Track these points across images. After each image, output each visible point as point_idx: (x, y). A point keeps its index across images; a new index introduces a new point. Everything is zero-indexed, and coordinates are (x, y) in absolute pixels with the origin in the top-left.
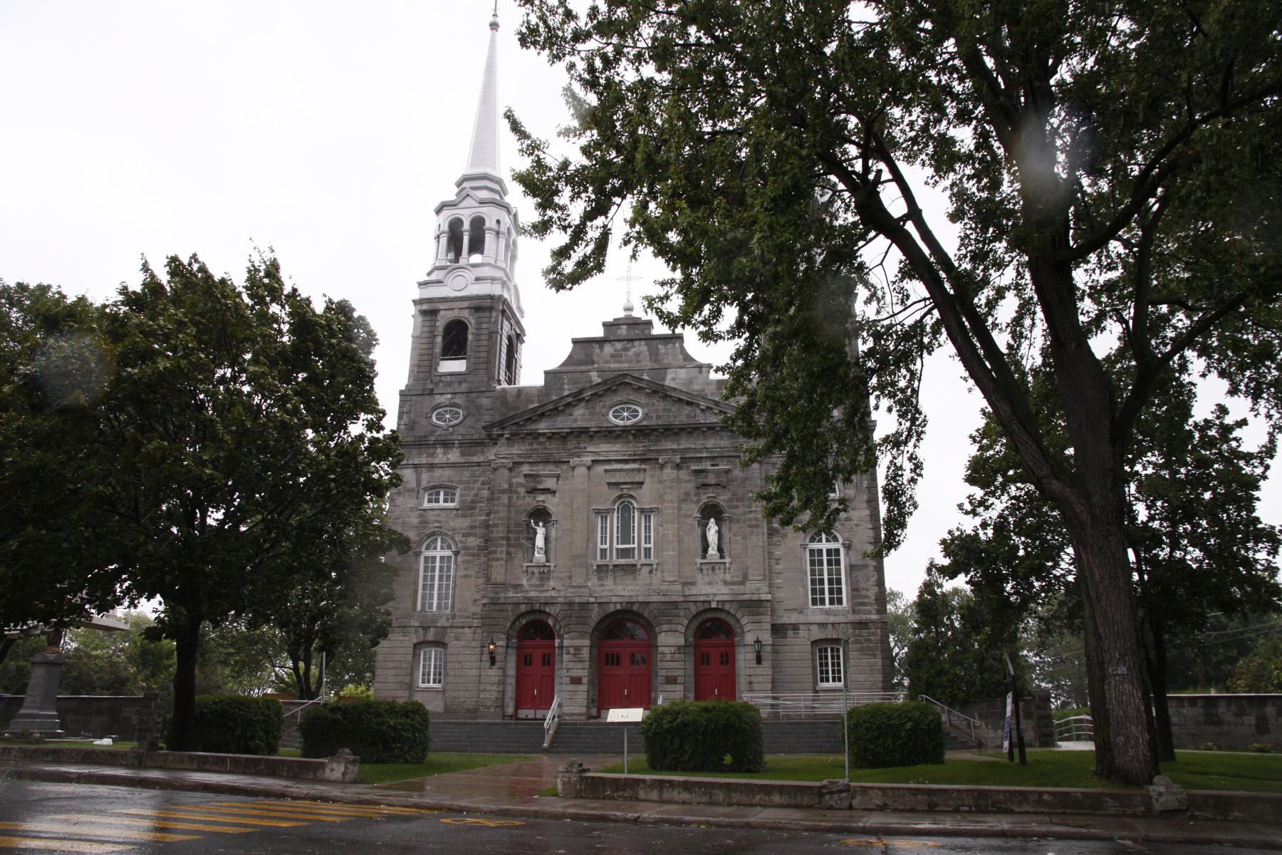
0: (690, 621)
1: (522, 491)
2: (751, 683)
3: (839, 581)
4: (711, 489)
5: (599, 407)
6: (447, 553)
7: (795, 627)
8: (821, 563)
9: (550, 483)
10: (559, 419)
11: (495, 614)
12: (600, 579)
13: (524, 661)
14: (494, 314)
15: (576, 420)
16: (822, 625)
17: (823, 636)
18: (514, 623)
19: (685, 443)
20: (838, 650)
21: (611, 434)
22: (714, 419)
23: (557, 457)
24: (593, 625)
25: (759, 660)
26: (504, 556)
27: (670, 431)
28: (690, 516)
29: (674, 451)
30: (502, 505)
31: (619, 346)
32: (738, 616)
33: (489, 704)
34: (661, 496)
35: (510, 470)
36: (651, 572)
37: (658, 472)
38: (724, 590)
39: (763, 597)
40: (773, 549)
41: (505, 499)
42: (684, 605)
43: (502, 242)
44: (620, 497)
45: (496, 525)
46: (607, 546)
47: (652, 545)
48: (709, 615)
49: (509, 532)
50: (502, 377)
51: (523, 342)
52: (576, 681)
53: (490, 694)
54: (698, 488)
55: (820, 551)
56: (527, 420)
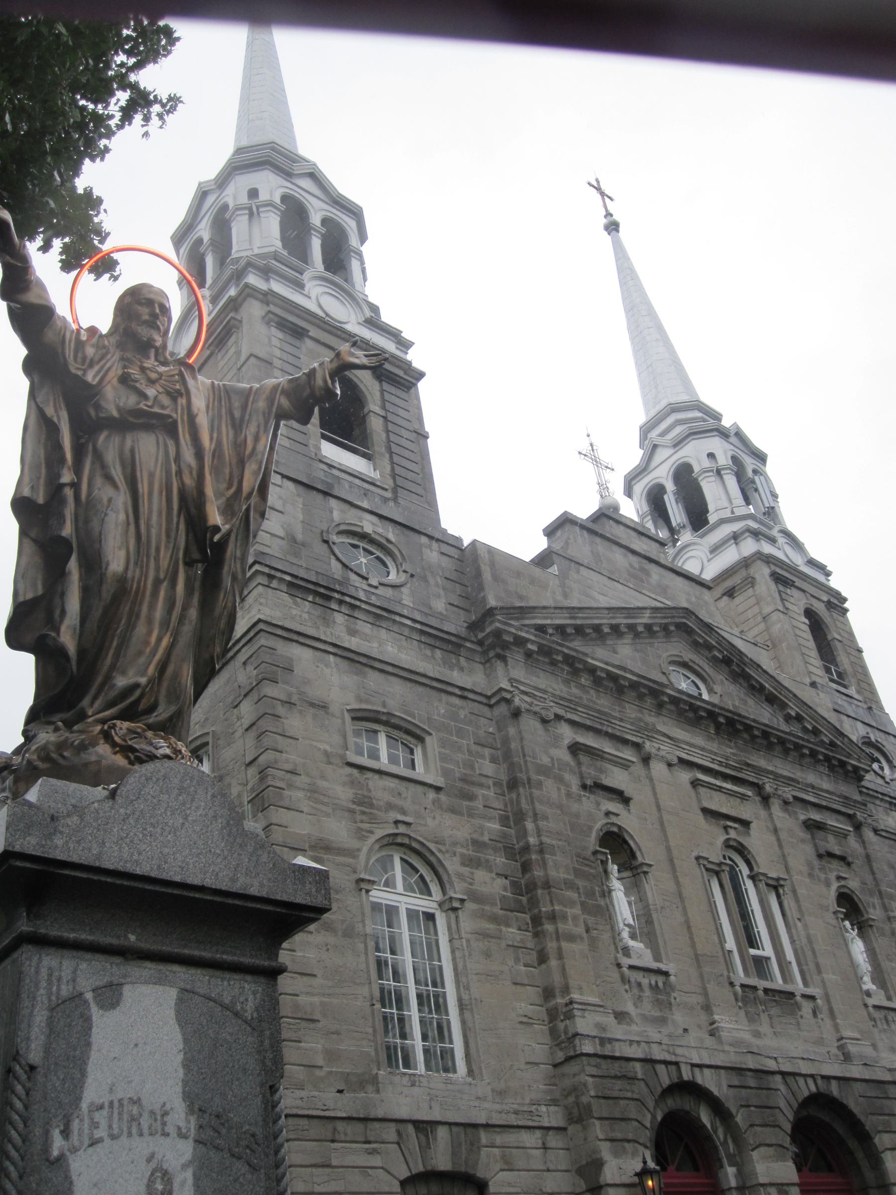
9: (617, 778)
26: (581, 930)
54: (820, 856)
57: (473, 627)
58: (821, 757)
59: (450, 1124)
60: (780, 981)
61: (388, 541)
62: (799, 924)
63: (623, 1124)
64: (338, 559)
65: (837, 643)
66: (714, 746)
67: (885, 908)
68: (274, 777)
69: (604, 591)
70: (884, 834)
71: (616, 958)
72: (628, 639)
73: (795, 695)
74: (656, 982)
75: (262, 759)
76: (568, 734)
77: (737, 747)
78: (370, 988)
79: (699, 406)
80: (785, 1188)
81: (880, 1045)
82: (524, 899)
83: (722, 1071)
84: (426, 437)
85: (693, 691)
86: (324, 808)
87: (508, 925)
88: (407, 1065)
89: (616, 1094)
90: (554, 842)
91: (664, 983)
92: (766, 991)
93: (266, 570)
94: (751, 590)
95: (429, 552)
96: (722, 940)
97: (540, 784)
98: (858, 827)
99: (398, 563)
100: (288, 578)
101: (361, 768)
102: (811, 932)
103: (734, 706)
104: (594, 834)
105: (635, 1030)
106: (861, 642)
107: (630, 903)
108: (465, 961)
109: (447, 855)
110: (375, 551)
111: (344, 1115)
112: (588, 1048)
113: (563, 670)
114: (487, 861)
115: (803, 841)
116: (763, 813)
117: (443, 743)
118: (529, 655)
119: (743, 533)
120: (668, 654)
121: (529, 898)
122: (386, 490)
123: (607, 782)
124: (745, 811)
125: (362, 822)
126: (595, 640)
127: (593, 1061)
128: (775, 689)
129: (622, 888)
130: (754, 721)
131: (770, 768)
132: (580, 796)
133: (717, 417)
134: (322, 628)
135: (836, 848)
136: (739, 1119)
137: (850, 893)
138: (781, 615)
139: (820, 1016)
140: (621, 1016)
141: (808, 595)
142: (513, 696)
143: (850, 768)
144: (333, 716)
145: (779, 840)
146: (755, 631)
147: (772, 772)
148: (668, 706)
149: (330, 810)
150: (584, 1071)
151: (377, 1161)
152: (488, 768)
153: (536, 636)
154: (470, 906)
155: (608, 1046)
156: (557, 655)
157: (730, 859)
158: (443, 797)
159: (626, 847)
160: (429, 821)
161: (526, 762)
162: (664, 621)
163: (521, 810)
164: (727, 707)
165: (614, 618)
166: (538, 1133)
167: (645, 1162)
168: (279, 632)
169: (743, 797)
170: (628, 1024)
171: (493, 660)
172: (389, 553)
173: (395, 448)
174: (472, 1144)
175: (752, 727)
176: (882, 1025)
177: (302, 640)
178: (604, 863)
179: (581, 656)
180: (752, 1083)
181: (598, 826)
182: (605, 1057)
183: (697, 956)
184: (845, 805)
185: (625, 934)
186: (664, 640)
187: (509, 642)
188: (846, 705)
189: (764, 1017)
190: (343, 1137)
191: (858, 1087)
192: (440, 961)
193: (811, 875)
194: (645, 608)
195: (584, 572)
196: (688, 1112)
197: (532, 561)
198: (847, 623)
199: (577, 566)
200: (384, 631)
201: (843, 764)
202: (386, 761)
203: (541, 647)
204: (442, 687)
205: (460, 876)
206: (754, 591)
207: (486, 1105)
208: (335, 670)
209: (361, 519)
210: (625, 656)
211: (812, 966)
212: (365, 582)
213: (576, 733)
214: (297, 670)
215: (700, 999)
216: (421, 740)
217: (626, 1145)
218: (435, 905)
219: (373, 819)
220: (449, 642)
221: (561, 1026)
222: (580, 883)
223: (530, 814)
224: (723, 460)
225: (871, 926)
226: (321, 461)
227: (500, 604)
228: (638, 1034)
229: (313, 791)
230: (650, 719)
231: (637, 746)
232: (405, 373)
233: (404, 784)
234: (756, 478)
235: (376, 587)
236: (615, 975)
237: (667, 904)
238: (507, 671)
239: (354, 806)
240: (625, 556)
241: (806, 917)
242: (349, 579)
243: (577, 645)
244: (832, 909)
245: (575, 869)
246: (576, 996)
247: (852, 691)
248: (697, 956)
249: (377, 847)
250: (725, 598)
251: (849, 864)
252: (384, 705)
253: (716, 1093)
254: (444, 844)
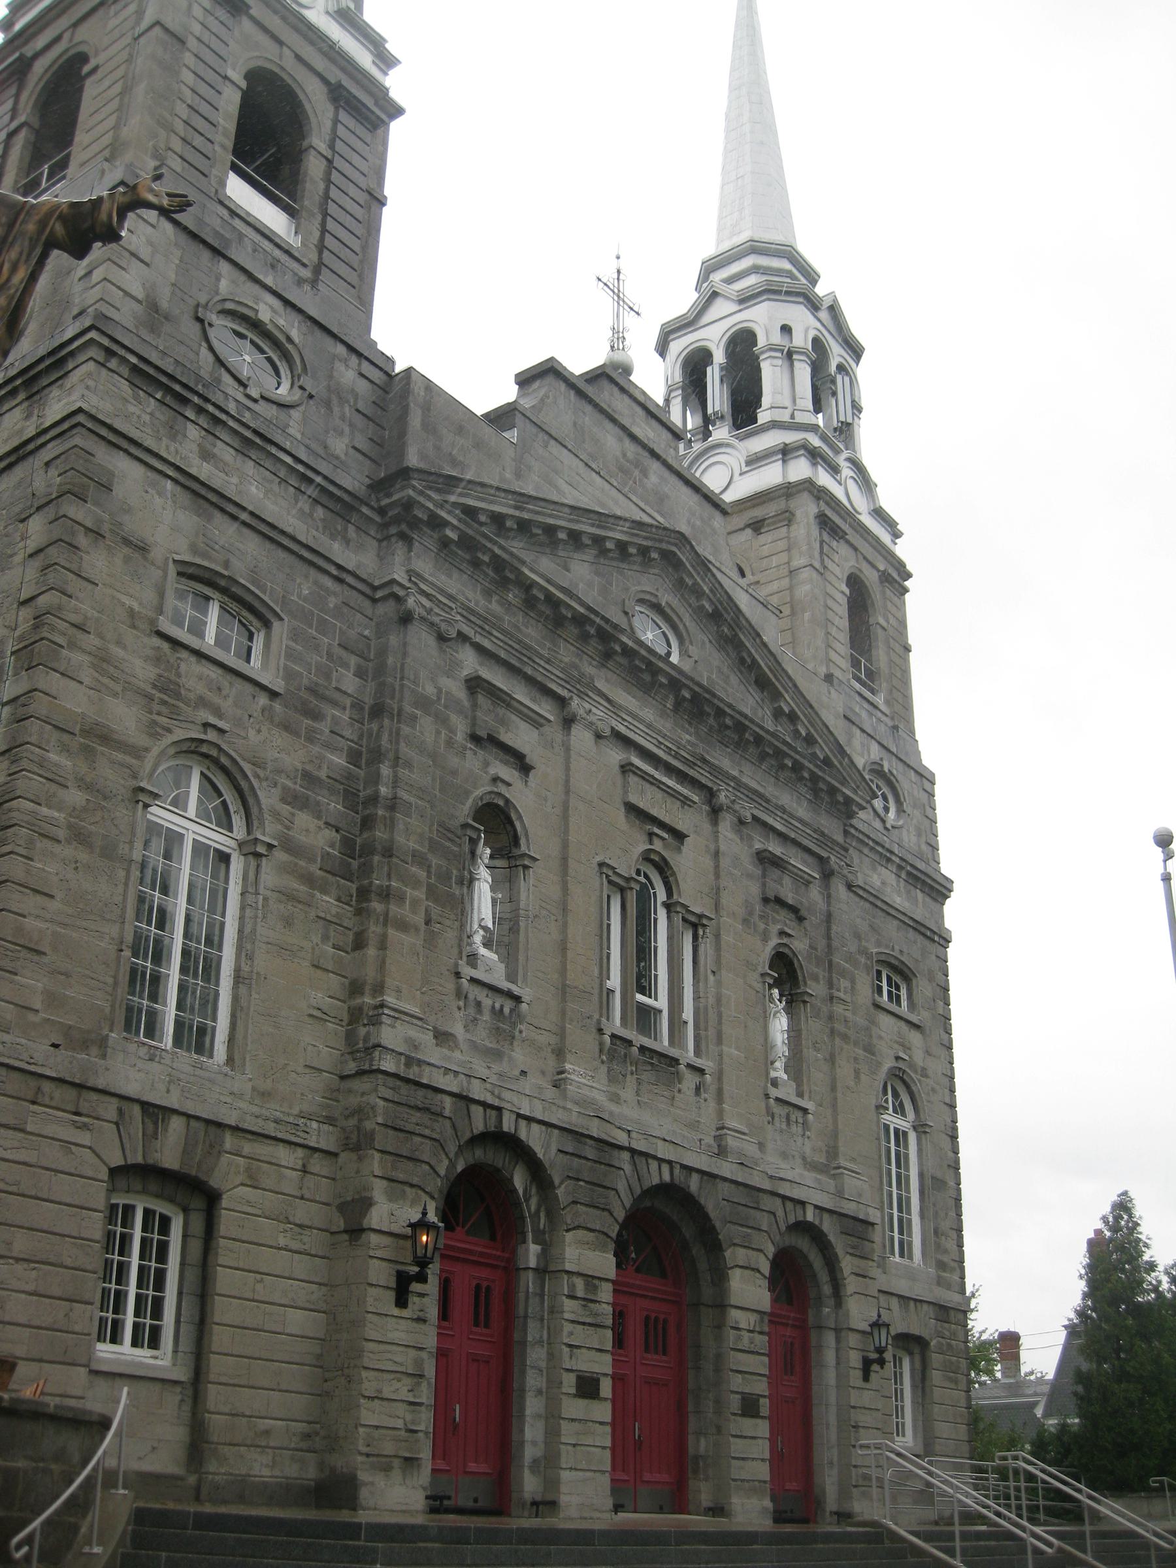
6: (217, 839)
9: (521, 737)
12: (612, 1079)
26: (419, 919)
27: (738, 733)
32: (840, 1250)
33: (389, 1448)
38: (809, 1177)
42: (768, 1203)
52: (587, 1387)
54: (766, 900)
57: (379, 486)
58: (806, 775)
59: (189, 1116)
60: (666, 1043)
61: (289, 339)
62: (711, 978)
63: (411, 1164)
64: (211, 349)
65: (880, 631)
66: (666, 725)
67: (831, 985)
68: (53, 628)
69: (574, 484)
70: (861, 892)
71: (457, 965)
72: (589, 554)
73: (795, 686)
74: (502, 1006)
75: (41, 599)
76: (469, 662)
78: (122, 930)
79: (790, 254)
80: (596, 1282)
81: (770, 1146)
82: (355, 864)
83: (556, 1131)
84: (382, 202)
85: (661, 650)
86: (111, 684)
87: (324, 891)
88: (151, 1032)
89: (409, 1127)
90: (412, 799)
91: (512, 1010)
92: (642, 1049)
93: (106, 342)
94: (784, 529)
95: (343, 368)
96: (605, 973)
97: (414, 718)
98: (827, 875)
99: (296, 373)
100: (134, 360)
101: (175, 643)
102: (724, 991)
103: (709, 678)
104: (471, 800)
105: (457, 1058)
106: (913, 638)
107: (494, 901)
108: (255, 923)
109: (265, 784)
110: (266, 349)
111: (54, 1075)
112: (388, 1064)
113: (486, 575)
114: (318, 803)
115: (750, 876)
116: (707, 827)
117: (295, 635)
118: (445, 543)
119: (797, 448)
120: (639, 588)
121: (359, 866)
122: (304, 265)
123: (507, 738)
124: (682, 820)
125: (159, 714)
126: (541, 545)
127: (391, 1081)
128: (771, 670)
129: (490, 880)
130: (730, 706)
131: (735, 773)
132: (465, 748)
133: (812, 277)
134: (165, 441)
135: (790, 895)
136: (560, 1192)
137: (791, 955)
138: (815, 575)
139: (704, 1095)
140: (442, 1037)
141: (861, 557)
142: (407, 595)
143: (841, 799)
144: (153, 564)
145: (717, 867)
146: (775, 586)
147: (734, 778)
148: (619, 659)
149: (118, 688)
150: (376, 1090)
151: (85, 1138)
152: (350, 683)
153: (460, 520)
154: (280, 855)
155: (416, 1069)
156: (484, 553)
157: (646, 876)
158: (277, 706)
159: (509, 828)
160: (252, 733)
161: (402, 686)
162: (645, 543)
163: (380, 746)
164: (697, 678)
165: (578, 522)
166: (300, 1152)
167: (424, 1214)
168: (104, 432)
169: (685, 802)
170: (451, 1049)
171: (393, 540)
172: (286, 356)
173: (332, 208)
174: (211, 1146)
175: (724, 713)
176: (780, 1124)
177: (133, 450)
178: (474, 842)
179: (516, 563)
180: (590, 1153)
181: (479, 792)
182: (408, 1081)
183: (564, 986)
185: (478, 939)
186: (639, 568)
187: (420, 520)
188: (864, 714)
189: (631, 1081)
190: (47, 1101)
191: (724, 1189)
192: (223, 915)
193: (745, 921)
194: (626, 520)
195: (554, 447)
196: (498, 1170)
197: (487, 416)
198: (901, 607)
199: (546, 437)
200: (252, 463)
201: (833, 791)
202: (212, 642)
203: (463, 537)
204: (311, 558)
205: (276, 814)
206: (788, 532)
207: (242, 1105)
208: (169, 502)
209: (257, 299)
210: (579, 578)
211: (712, 1032)
212: (241, 389)
213: (481, 664)
214: (118, 491)
215: (553, 1040)
216: (267, 624)
217: (408, 1189)
218: (233, 844)
219: (174, 713)
220: (339, 499)
221: (362, 1031)
222: (435, 861)
223: (391, 755)
224: (801, 340)
225: (805, 1002)
226: (221, 203)
227: (422, 465)
228: (460, 1063)
229: (102, 660)
230: (589, 669)
231: (562, 702)
232: (376, 104)
233: (229, 677)
234: (839, 378)
235: (255, 401)
236: (450, 986)
237: (544, 912)
238: (409, 559)
239: (154, 692)
240: (620, 440)
241: (723, 972)
242: (219, 381)
243: (517, 547)
244: (760, 970)
245: (431, 839)
246: (390, 999)
247: (879, 700)
248: (564, 986)
249: (172, 751)
250: (749, 531)
251: (801, 919)
252: (226, 564)
253: (540, 1156)
254: (265, 769)
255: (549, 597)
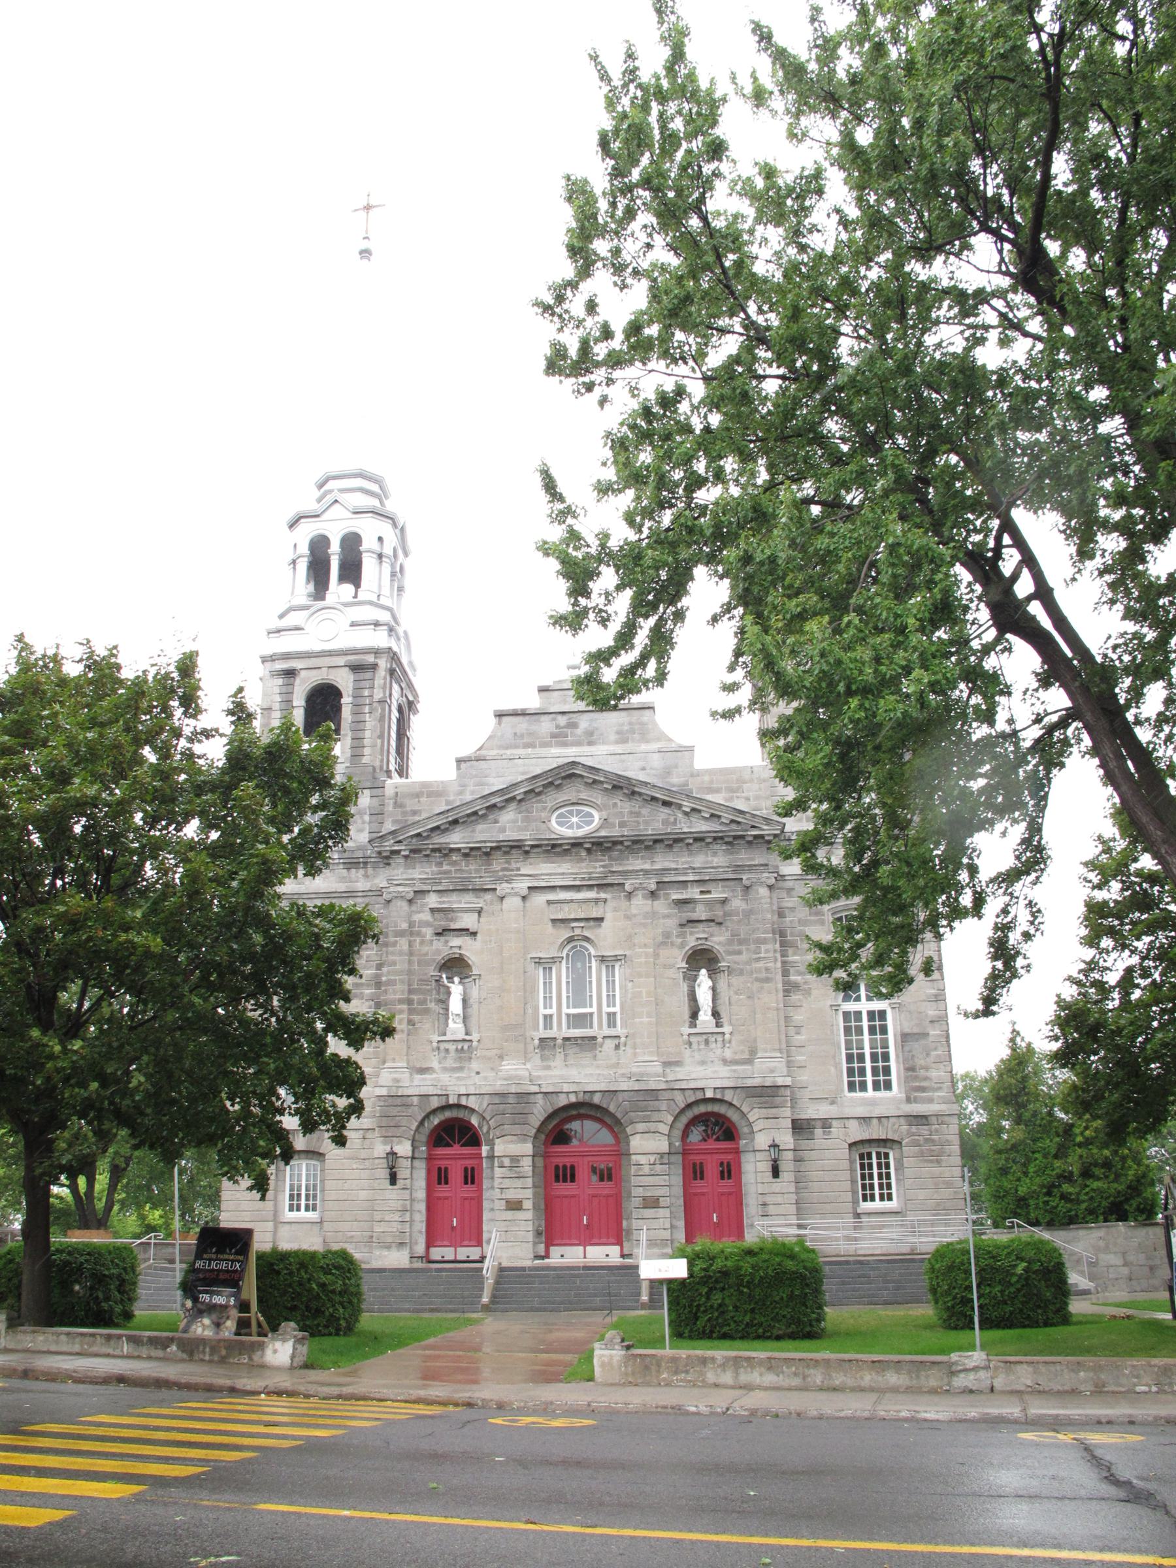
0: (676, 1118)
1: (428, 932)
2: (764, 1205)
3: (886, 1057)
4: (701, 926)
5: (535, 806)
7: (826, 1123)
8: (859, 1031)
9: (467, 921)
10: (479, 827)
11: (394, 1111)
12: (543, 1058)
13: (438, 1176)
14: (382, 672)
15: (503, 830)
16: (865, 1120)
17: (865, 1136)
18: (422, 1123)
19: (662, 861)
20: (887, 1155)
21: (555, 849)
22: (701, 826)
23: (478, 883)
24: (537, 1124)
25: (776, 1172)
28: (671, 966)
29: (646, 872)
30: (401, 953)
31: (562, 720)
32: (745, 1109)
33: (389, 1240)
34: (629, 938)
35: (410, 901)
36: (617, 1047)
37: (624, 903)
39: (780, 1081)
40: (791, 1012)
41: (403, 944)
42: (667, 1095)
43: (387, 568)
44: (570, 940)
45: (390, 983)
46: (553, 1011)
47: (617, 1009)
48: (702, 1109)
49: (410, 992)
50: (392, 767)
51: (416, 712)
52: (514, 1206)
53: (390, 1226)
55: (858, 1014)
56: (433, 830)
77: (611, 858)
184: (734, 872)
203: (412, 851)
255: (472, 849)
